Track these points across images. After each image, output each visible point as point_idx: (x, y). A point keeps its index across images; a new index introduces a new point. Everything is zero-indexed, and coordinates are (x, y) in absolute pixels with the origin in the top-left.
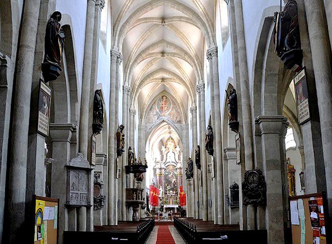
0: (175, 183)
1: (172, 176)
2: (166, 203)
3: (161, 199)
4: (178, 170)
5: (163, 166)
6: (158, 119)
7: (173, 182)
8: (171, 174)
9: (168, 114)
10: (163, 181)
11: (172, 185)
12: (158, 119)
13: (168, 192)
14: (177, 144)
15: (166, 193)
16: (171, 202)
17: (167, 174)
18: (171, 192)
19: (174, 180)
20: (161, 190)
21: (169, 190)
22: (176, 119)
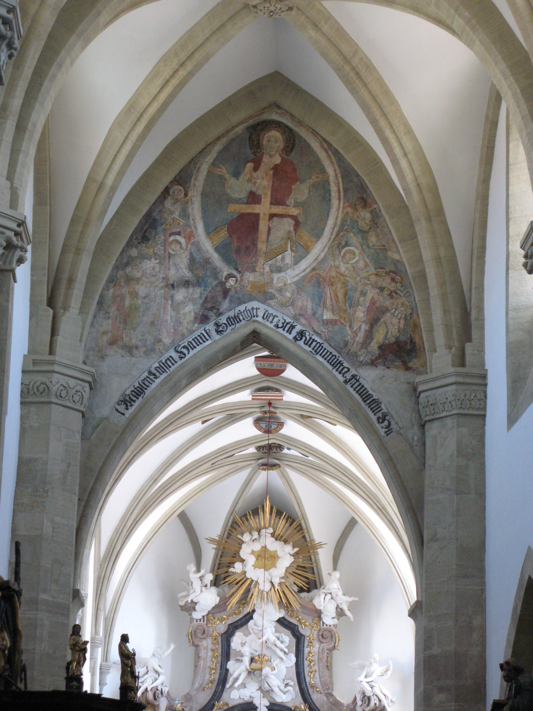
6: (204, 319)
9: (300, 286)
12: (204, 319)
22: (373, 322)
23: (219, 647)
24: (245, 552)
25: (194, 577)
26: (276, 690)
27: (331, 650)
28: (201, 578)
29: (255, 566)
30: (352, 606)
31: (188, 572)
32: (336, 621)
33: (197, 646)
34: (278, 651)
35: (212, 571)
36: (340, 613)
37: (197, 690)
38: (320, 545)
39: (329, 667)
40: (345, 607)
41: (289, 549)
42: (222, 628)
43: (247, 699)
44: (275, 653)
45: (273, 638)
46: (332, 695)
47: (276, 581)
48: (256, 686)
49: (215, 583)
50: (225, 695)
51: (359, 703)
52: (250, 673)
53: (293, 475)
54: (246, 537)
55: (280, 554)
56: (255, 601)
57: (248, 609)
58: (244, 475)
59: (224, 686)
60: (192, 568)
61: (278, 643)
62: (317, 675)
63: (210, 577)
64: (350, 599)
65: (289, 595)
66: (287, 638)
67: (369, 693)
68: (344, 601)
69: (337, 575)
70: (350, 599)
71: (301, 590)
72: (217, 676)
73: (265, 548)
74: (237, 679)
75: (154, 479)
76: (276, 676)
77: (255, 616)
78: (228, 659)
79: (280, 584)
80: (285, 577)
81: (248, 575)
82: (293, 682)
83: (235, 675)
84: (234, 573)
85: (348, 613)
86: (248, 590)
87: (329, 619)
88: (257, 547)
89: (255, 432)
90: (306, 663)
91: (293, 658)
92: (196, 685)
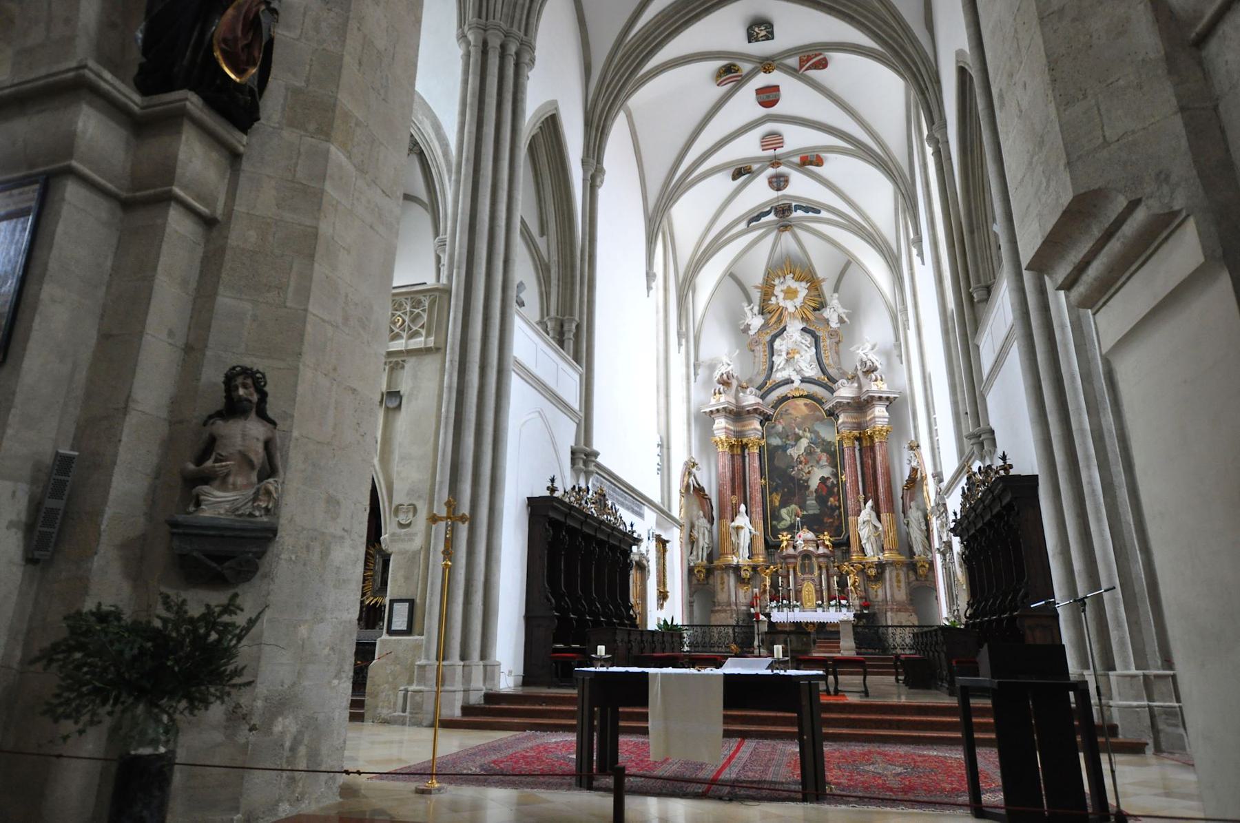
0: (828, 489)
1: (809, 452)
2: (777, 595)
3: (746, 574)
4: (842, 418)
5: (750, 399)
7: (814, 483)
8: (804, 443)
10: (755, 479)
11: (811, 502)
13: (785, 538)
14: (827, 288)
15: (772, 546)
16: (809, 589)
17: (776, 441)
18: (807, 535)
19: (818, 474)
20: (746, 526)
21: (792, 529)
23: (767, 349)
24: (777, 291)
25: (747, 309)
26: (805, 369)
27: (838, 343)
28: (751, 309)
29: (784, 299)
30: (848, 315)
31: (743, 308)
32: (839, 325)
33: (753, 351)
34: (803, 346)
35: (759, 306)
36: (841, 320)
37: (756, 376)
38: (824, 280)
39: (837, 353)
40: (844, 316)
41: (804, 284)
42: (768, 338)
43: (787, 377)
44: (801, 347)
45: (799, 339)
46: (841, 368)
47: (798, 305)
48: (791, 369)
49: (762, 312)
50: (773, 376)
51: (859, 368)
52: (787, 361)
53: (801, 234)
54: (777, 282)
55: (799, 289)
56: (787, 320)
57: (783, 325)
58: (772, 237)
59: (772, 371)
60: (745, 304)
61: (803, 341)
62: (830, 358)
63: (756, 309)
64: (846, 311)
65: (807, 313)
66: (809, 339)
67: (865, 359)
68: (841, 311)
69: (836, 295)
70: (846, 311)
71: (815, 309)
72: (767, 366)
73: (789, 287)
74: (779, 365)
75: (708, 230)
76: (804, 360)
77: (787, 328)
78: (773, 355)
79: (801, 307)
80: (804, 302)
81: (780, 305)
82: (815, 364)
83: (778, 363)
84: (772, 304)
85: (846, 319)
86: (781, 314)
87: (834, 324)
88: (784, 287)
89: (773, 194)
90: (822, 352)
91: (814, 350)
92: (755, 372)
